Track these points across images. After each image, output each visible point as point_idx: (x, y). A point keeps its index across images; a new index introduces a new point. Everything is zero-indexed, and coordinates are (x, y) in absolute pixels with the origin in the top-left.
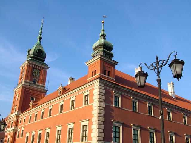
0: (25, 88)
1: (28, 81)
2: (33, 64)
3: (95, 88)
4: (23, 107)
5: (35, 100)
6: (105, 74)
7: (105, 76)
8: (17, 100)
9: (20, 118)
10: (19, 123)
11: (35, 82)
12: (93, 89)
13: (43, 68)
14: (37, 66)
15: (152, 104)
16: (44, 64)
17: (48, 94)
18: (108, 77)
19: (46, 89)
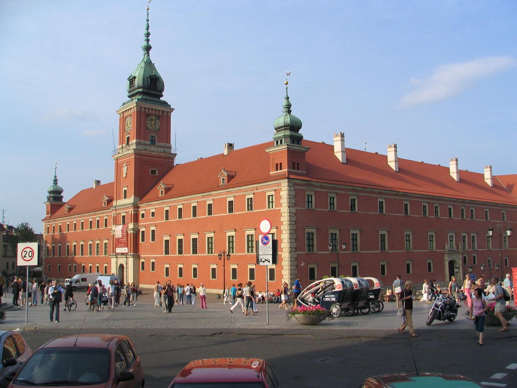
0: (140, 155)
1: (142, 141)
2: (145, 108)
3: (283, 188)
4: (143, 189)
5: (157, 174)
6: (294, 169)
7: (294, 171)
8: (125, 176)
9: (139, 209)
10: (140, 218)
11: (153, 142)
12: (280, 190)
13: (163, 112)
14: (152, 110)
15: (356, 195)
16: (165, 104)
17: (177, 161)
18: (298, 171)
19: (173, 152)
